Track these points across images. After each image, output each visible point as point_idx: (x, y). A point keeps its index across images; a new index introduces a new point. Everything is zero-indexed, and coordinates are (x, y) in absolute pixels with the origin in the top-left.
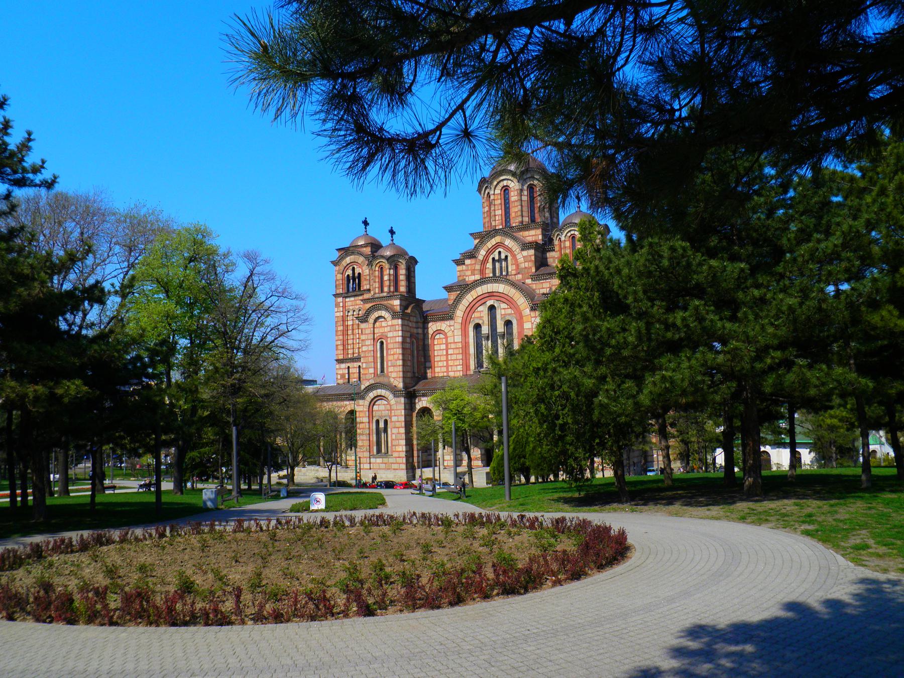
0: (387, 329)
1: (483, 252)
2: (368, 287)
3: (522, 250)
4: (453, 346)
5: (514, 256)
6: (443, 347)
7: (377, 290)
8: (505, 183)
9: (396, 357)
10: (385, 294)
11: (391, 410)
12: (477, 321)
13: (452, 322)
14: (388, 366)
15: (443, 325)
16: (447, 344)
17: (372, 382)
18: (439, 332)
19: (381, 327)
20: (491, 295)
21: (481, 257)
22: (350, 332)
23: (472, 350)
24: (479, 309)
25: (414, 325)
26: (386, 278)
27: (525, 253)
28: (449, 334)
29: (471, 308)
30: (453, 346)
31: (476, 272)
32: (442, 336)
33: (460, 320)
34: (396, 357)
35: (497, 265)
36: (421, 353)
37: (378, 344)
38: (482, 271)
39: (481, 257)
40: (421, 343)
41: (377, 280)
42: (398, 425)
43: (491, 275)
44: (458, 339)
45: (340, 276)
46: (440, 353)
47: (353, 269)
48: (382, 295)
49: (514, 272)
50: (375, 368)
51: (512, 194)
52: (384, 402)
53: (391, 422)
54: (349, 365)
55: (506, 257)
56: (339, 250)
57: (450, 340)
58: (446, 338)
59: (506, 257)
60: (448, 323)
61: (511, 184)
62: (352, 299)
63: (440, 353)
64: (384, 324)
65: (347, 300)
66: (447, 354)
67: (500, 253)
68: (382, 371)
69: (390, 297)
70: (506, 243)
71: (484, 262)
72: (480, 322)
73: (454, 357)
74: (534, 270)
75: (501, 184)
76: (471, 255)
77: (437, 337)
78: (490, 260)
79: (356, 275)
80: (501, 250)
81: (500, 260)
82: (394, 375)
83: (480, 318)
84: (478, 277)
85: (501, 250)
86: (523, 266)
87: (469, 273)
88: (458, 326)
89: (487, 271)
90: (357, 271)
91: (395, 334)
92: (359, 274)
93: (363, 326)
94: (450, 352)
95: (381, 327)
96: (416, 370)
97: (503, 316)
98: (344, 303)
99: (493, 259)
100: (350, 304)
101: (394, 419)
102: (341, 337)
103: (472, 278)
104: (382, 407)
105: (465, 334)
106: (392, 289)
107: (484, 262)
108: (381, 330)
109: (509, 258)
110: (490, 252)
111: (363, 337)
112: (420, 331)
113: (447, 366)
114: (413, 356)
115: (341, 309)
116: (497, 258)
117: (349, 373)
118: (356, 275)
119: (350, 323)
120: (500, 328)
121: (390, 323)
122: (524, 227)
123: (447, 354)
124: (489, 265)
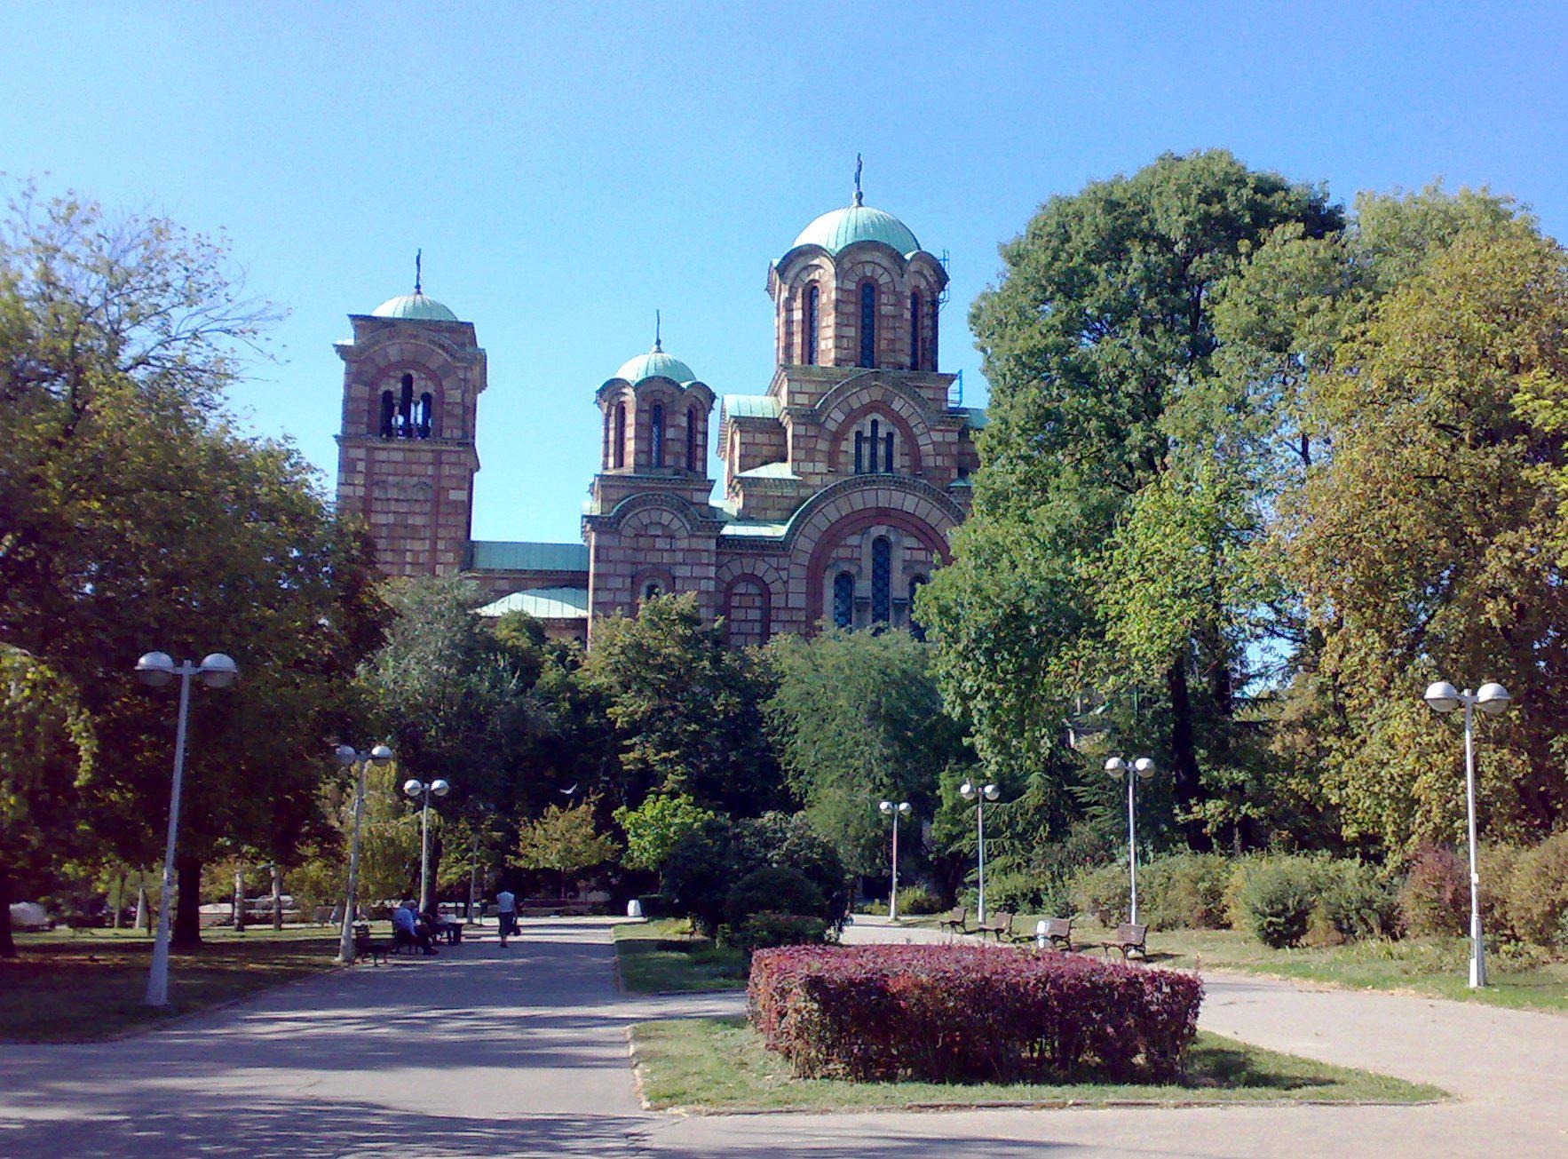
0: (667, 558)
4: (783, 616)
5: (910, 438)
6: (755, 614)
10: (668, 474)
12: (845, 567)
13: (784, 562)
18: (750, 578)
19: (654, 549)
20: (883, 514)
24: (853, 540)
27: (937, 437)
28: (776, 587)
29: (833, 536)
30: (783, 616)
31: (818, 456)
32: (753, 589)
33: (805, 560)
35: (866, 449)
39: (832, 426)
44: (798, 600)
45: (362, 391)
47: (408, 381)
51: (884, 299)
55: (890, 435)
56: (353, 317)
57: (777, 601)
58: (766, 593)
59: (890, 435)
60: (774, 562)
61: (885, 279)
62: (398, 456)
64: (660, 543)
65: (382, 456)
70: (896, 406)
71: (837, 437)
72: (854, 570)
75: (859, 270)
77: (740, 589)
78: (852, 437)
80: (879, 417)
83: (851, 560)
85: (879, 417)
86: (930, 462)
88: (799, 572)
89: (842, 458)
91: (698, 571)
95: (654, 549)
97: (908, 565)
98: (371, 462)
99: (859, 434)
109: (897, 440)
115: (360, 480)
121: (684, 544)
124: (849, 446)
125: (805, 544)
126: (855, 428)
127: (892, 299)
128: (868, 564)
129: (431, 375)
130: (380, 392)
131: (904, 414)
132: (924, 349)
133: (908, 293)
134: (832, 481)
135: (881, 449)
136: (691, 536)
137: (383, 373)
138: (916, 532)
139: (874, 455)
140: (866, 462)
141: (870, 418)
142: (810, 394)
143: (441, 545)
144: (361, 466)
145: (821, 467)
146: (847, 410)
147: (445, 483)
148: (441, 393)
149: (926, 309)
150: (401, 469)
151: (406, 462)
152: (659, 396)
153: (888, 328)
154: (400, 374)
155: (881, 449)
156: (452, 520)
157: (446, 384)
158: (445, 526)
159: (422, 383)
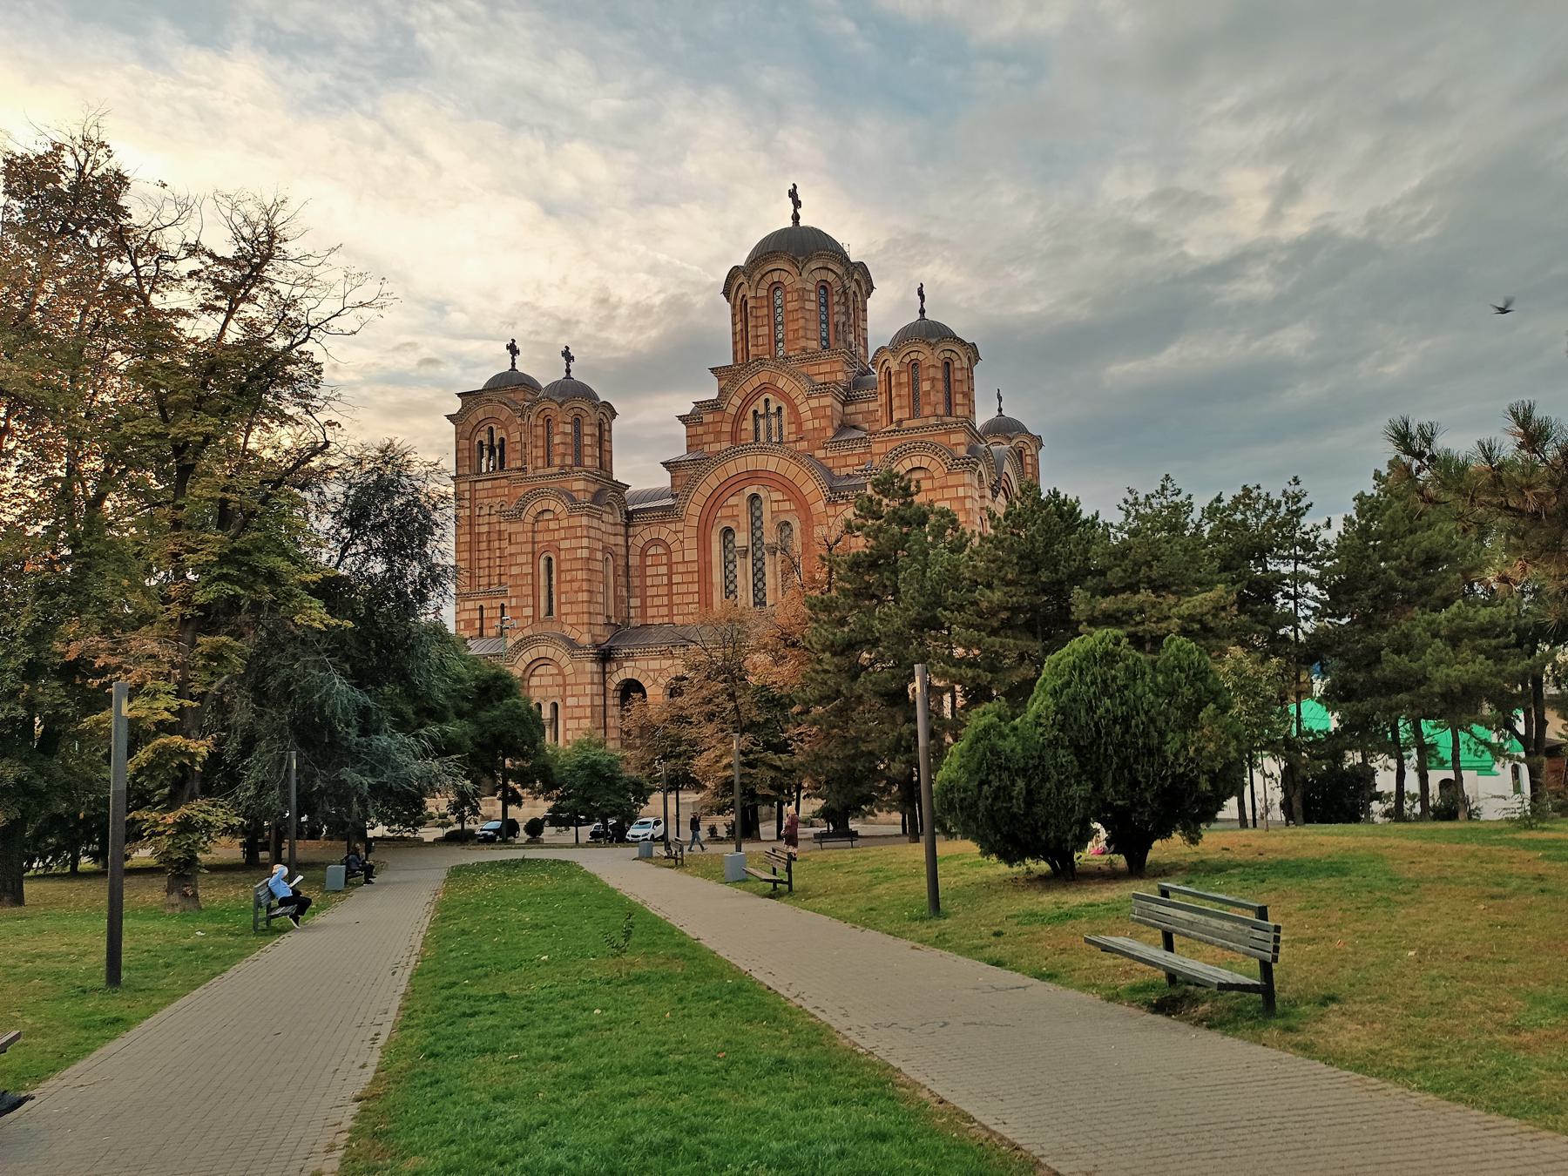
1: (737, 401)
2: (519, 464)
3: (809, 397)
4: (681, 568)
5: (794, 408)
6: (664, 570)
7: (540, 462)
8: (776, 277)
9: (576, 585)
10: (556, 470)
11: (565, 685)
12: (726, 523)
13: (680, 526)
14: (560, 604)
15: (664, 533)
16: (670, 565)
17: (528, 632)
18: (656, 542)
20: (753, 476)
22: (484, 546)
23: (717, 576)
24: (732, 501)
25: (610, 529)
26: (557, 439)
27: (814, 403)
29: (716, 500)
30: (681, 568)
31: (724, 437)
32: (660, 550)
34: (576, 585)
35: (762, 422)
36: (622, 580)
37: (543, 563)
38: (734, 436)
39: (732, 410)
40: (622, 562)
41: (540, 443)
42: (577, 713)
44: (692, 555)
46: (657, 581)
48: (549, 471)
49: (793, 437)
50: (535, 607)
52: (552, 670)
53: (565, 707)
54: (479, 603)
55: (779, 409)
56: (459, 395)
57: (676, 557)
58: (669, 553)
59: (779, 409)
60: (672, 527)
62: (488, 484)
63: (657, 581)
64: (552, 525)
65: (479, 486)
66: (670, 584)
67: (767, 401)
68: (550, 613)
69: (564, 472)
70: (780, 384)
71: (739, 418)
73: (684, 588)
74: (830, 433)
75: (769, 279)
76: (713, 406)
77: (652, 551)
78: (750, 415)
79: (496, 442)
81: (766, 415)
82: (572, 619)
84: (726, 445)
86: (809, 425)
87: (711, 437)
91: (575, 543)
92: (502, 440)
93: (515, 527)
94: (676, 579)
96: (612, 613)
98: (473, 491)
100: (483, 494)
101: (570, 701)
102: (466, 555)
103: (716, 447)
104: (547, 681)
105: (704, 547)
106: (569, 460)
107: (739, 418)
108: (548, 536)
109: (784, 412)
110: (748, 400)
111: (513, 549)
112: (621, 540)
113: (670, 605)
114: (607, 586)
116: (761, 411)
117: (481, 619)
118: (496, 442)
119: (485, 529)
120: (770, 537)
121: (564, 523)
122: (810, 357)
123: (670, 584)
124: (748, 425)
125: (694, 509)
126: (752, 408)
127: (795, 296)
132: (836, 331)
133: (810, 287)
135: (774, 422)
138: (778, 486)
139: (769, 429)
140: (762, 437)
141: (763, 398)
144: (467, 495)
149: (836, 299)
152: (547, 412)
155: (774, 422)
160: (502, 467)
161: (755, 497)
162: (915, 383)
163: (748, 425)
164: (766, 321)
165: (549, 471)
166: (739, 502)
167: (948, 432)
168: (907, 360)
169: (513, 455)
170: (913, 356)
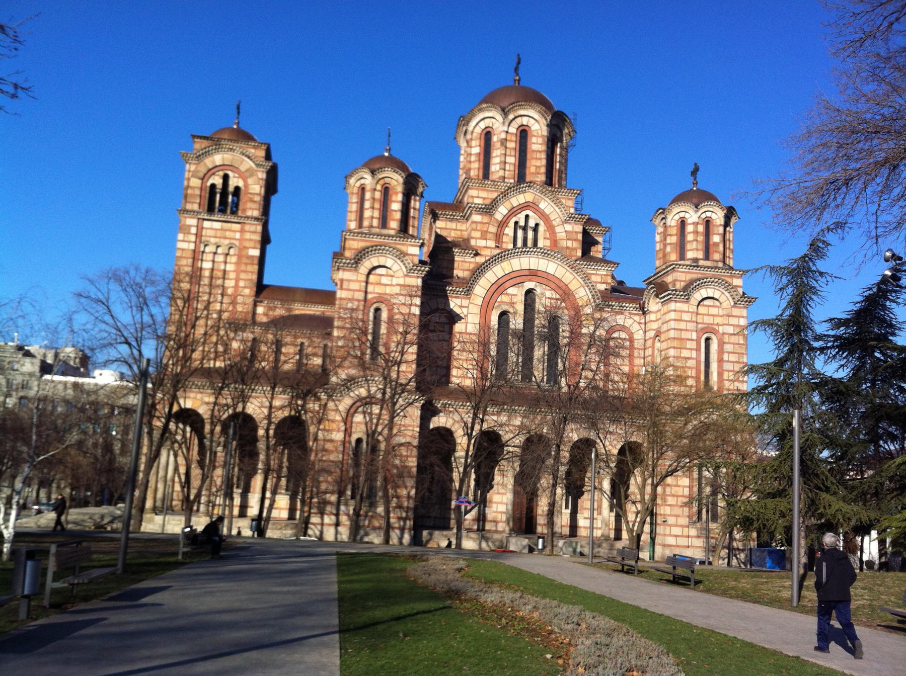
0: (388, 290)
2: (256, 213)
3: (566, 222)
5: (551, 228)
7: (375, 223)
8: (525, 121)
10: (392, 232)
12: (505, 308)
19: (380, 284)
20: (533, 274)
21: (499, 216)
24: (511, 291)
27: (568, 227)
29: (499, 287)
31: (489, 236)
33: (479, 301)
35: (520, 233)
39: (499, 216)
43: (511, 246)
47: (226, 178)
51: (534, 140)
55: (537, 225)
62: (217, 225)
64: (384, 280)
65: (207, 224)
70: (542, 205)
71: (502, 224)
75: (519, 121)
79: (231, 189)
86: (564, 244)
87: (477, 234)
88: (476, 310)
89: (505, 239)
90: (234, 182)
92: (237, 189)
98: (200, 228)
99: (516, 223)
103: (482, 243)
108: (379, 289)
109: (542, 228)
110: (513, 212)
115: (193, 238)
118: (231, 189)
124: (509, 231)
126: (514, 220)
128: (520, 307)
129: (241, 175)
130: (209, 184)
131: (547, 211)
134: (498, 251)
135: (530, 234)
136: (406, 276)
137: (211, 171)
138: (553, 286)
140: (520, 243)
142: (484, 199)
143: (242, 284)
144: (194, 230)
145: (492, 244)
146: (509, 207)
147: (247, 244)
148: (246, 185)
150: (219, 234)
151: (222, 229)
152: (387, 180)
153: (537, 159)
154: (221, 173)
155: (530, 234)
156: (249, 268)
157: (250, 181)
158: (245, 272)
159: (236, 180)
160: (234, 213)
161: (529, 292)
162: (707, 234)
163: (509, 231)
164: (513, 153)
165: (385, 231)
166: (517, 294)
167: (732, 276)
168: (703, 216)
169: (249, 205)
170: (708, 214)
